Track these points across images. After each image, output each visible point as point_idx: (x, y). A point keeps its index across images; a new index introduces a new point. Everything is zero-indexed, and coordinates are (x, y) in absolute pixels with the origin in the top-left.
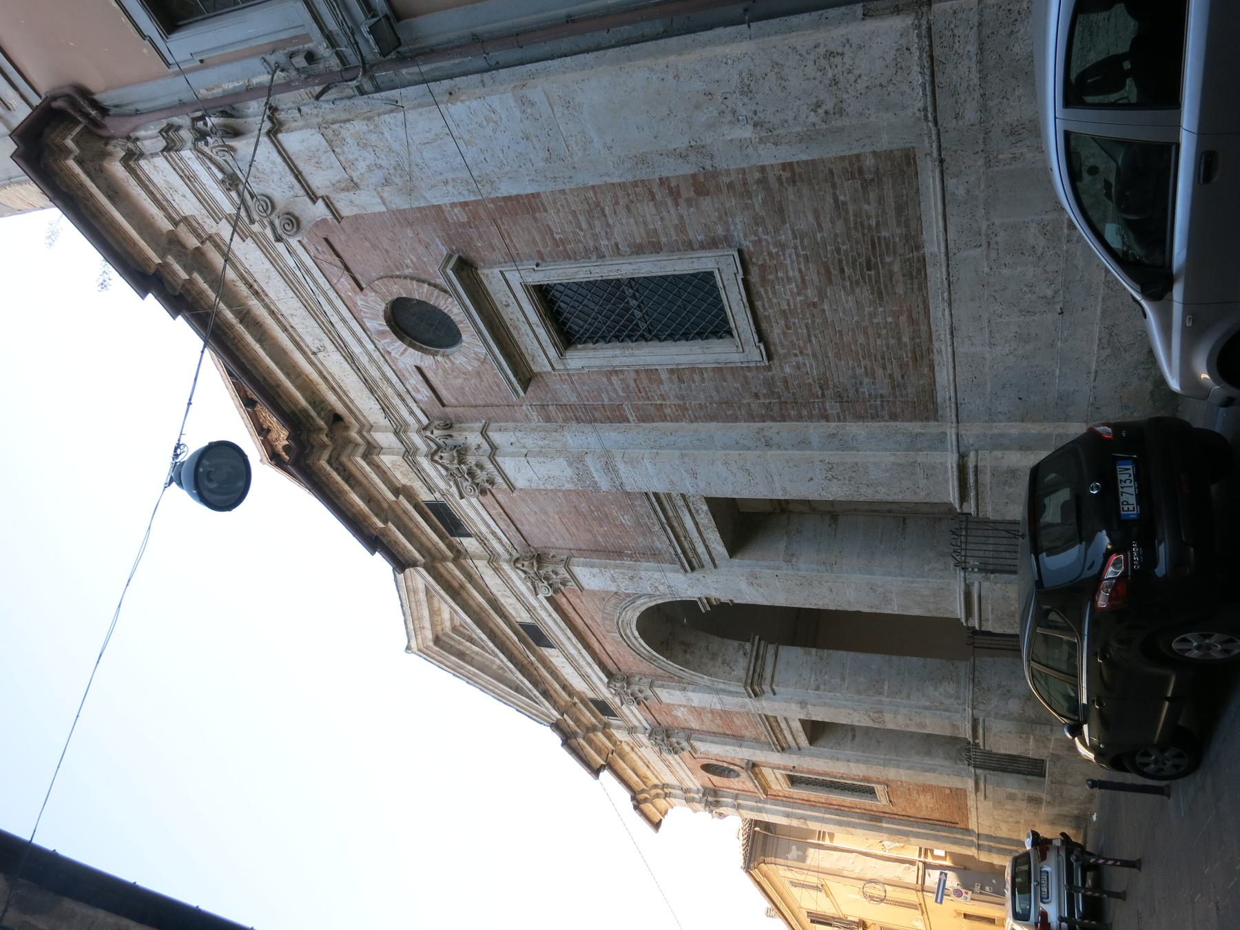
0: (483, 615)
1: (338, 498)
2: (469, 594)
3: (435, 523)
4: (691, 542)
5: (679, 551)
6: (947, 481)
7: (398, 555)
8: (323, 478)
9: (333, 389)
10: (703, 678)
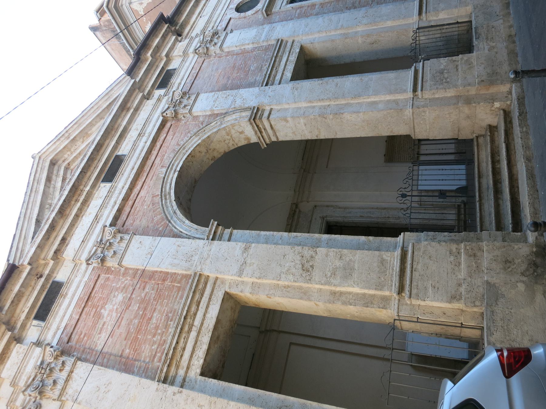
0: (113, 132)
1: (153, 36)
2: (125, 116)
3: (158, 81)
4: (277, 72)
5: (269, 73)
6: (414, 9)
7: (133, 72)
8: (160, 28)
9: (192, 27)
10: (184, 222)
